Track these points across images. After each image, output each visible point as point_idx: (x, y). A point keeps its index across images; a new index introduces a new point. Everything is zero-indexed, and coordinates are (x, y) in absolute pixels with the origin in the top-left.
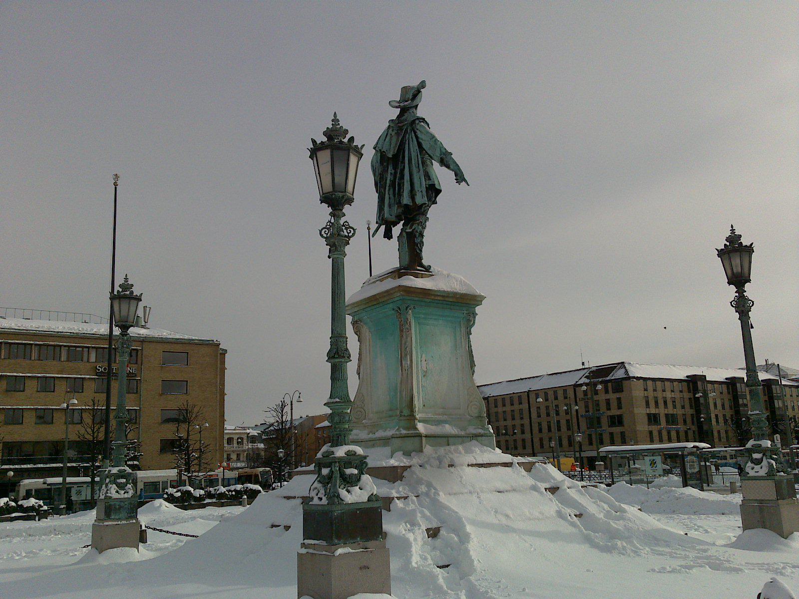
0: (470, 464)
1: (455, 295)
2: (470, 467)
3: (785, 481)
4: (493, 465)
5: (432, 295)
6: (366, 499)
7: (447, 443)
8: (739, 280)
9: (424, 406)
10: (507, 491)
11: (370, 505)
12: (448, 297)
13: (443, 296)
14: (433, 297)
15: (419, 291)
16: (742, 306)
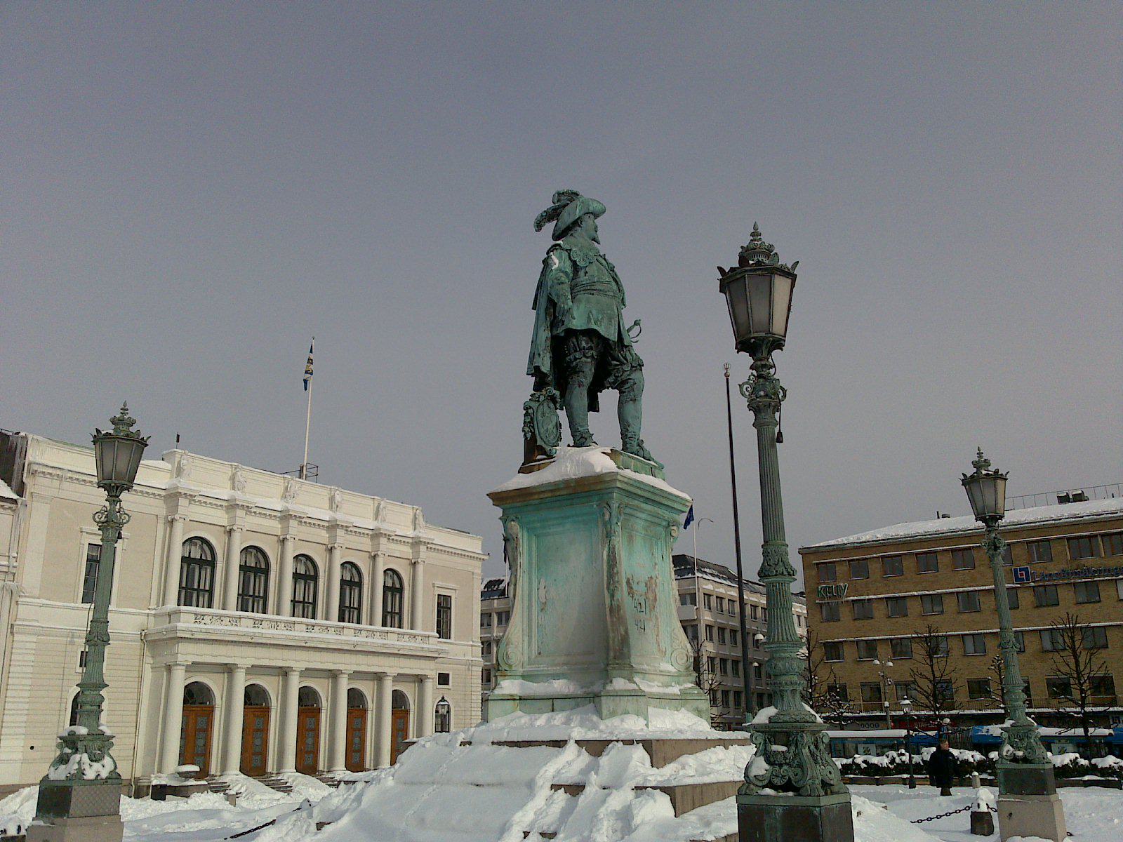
0: (496, 741)
1: (567, 483)
2: (495, 746)
3: (779, 810)
4: (536, 743)
5: (535, 493)
6: (63, 778)
7: (551, 708)
8: (758, 343)
9: (540, 653)
10: (489, 785)
11: (68, 784)
12: (559, 489)
13: (551, 491)
14: (536, 497)
15: (513, 494)
16: (765, 400)
